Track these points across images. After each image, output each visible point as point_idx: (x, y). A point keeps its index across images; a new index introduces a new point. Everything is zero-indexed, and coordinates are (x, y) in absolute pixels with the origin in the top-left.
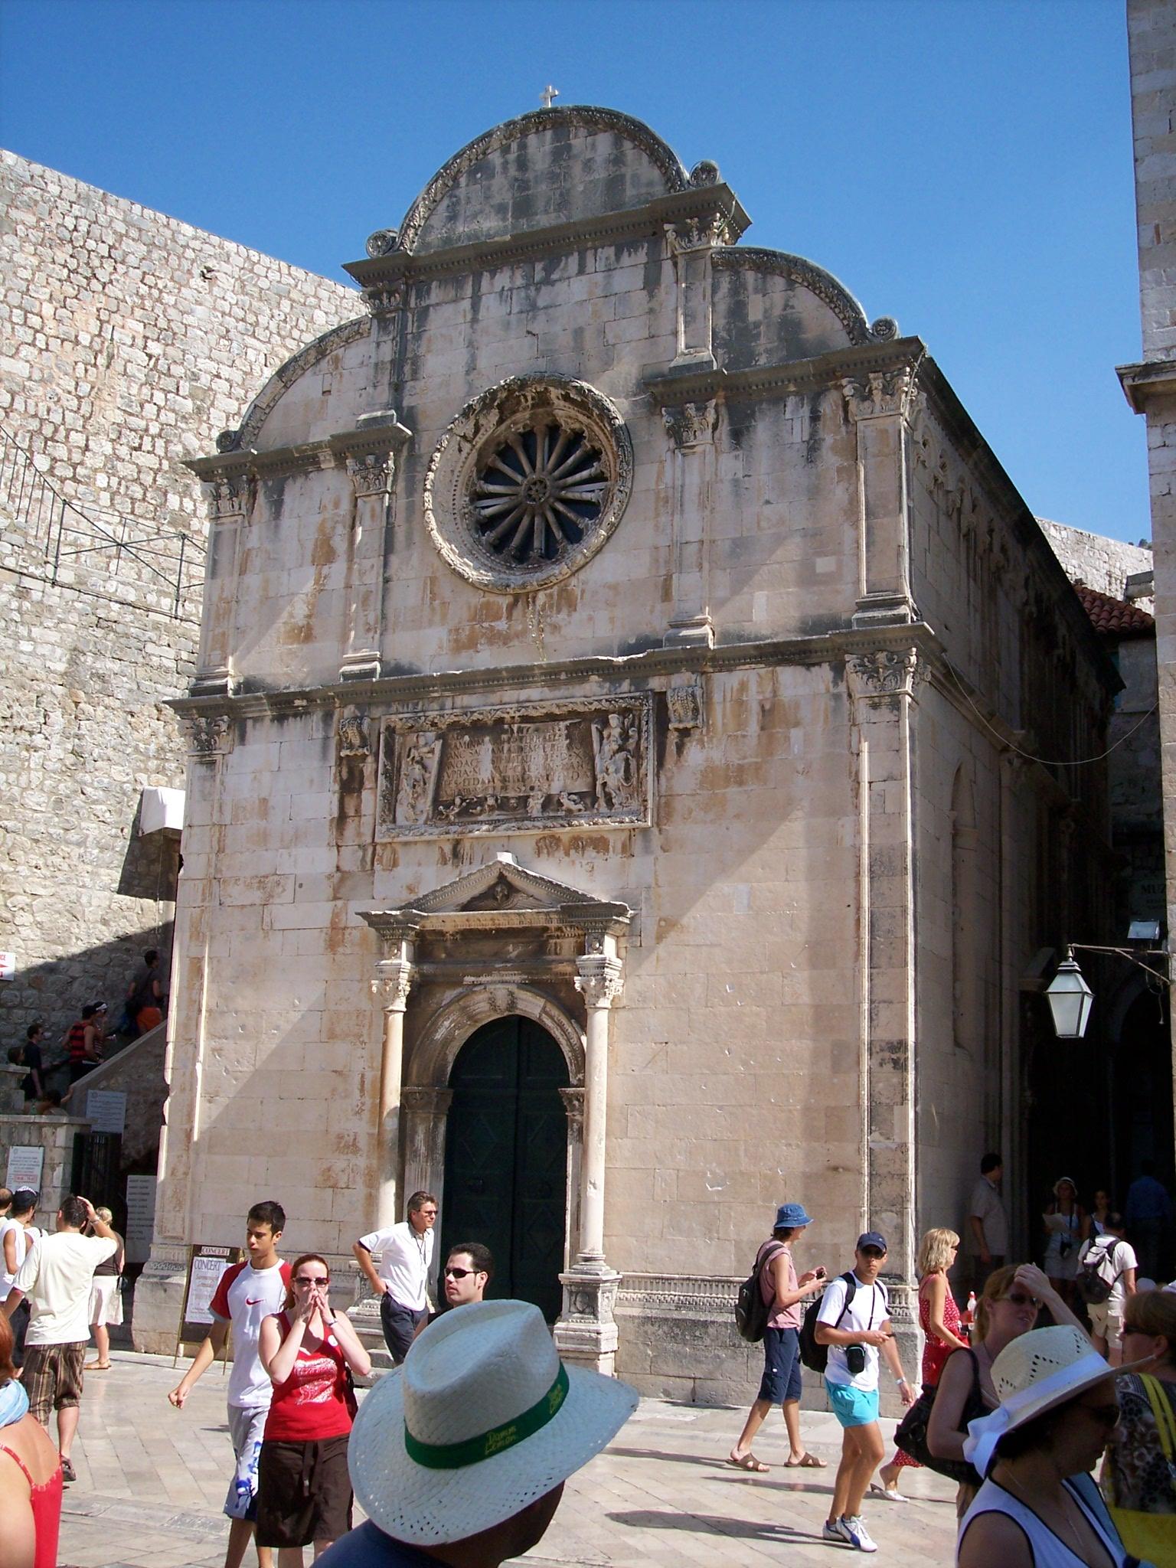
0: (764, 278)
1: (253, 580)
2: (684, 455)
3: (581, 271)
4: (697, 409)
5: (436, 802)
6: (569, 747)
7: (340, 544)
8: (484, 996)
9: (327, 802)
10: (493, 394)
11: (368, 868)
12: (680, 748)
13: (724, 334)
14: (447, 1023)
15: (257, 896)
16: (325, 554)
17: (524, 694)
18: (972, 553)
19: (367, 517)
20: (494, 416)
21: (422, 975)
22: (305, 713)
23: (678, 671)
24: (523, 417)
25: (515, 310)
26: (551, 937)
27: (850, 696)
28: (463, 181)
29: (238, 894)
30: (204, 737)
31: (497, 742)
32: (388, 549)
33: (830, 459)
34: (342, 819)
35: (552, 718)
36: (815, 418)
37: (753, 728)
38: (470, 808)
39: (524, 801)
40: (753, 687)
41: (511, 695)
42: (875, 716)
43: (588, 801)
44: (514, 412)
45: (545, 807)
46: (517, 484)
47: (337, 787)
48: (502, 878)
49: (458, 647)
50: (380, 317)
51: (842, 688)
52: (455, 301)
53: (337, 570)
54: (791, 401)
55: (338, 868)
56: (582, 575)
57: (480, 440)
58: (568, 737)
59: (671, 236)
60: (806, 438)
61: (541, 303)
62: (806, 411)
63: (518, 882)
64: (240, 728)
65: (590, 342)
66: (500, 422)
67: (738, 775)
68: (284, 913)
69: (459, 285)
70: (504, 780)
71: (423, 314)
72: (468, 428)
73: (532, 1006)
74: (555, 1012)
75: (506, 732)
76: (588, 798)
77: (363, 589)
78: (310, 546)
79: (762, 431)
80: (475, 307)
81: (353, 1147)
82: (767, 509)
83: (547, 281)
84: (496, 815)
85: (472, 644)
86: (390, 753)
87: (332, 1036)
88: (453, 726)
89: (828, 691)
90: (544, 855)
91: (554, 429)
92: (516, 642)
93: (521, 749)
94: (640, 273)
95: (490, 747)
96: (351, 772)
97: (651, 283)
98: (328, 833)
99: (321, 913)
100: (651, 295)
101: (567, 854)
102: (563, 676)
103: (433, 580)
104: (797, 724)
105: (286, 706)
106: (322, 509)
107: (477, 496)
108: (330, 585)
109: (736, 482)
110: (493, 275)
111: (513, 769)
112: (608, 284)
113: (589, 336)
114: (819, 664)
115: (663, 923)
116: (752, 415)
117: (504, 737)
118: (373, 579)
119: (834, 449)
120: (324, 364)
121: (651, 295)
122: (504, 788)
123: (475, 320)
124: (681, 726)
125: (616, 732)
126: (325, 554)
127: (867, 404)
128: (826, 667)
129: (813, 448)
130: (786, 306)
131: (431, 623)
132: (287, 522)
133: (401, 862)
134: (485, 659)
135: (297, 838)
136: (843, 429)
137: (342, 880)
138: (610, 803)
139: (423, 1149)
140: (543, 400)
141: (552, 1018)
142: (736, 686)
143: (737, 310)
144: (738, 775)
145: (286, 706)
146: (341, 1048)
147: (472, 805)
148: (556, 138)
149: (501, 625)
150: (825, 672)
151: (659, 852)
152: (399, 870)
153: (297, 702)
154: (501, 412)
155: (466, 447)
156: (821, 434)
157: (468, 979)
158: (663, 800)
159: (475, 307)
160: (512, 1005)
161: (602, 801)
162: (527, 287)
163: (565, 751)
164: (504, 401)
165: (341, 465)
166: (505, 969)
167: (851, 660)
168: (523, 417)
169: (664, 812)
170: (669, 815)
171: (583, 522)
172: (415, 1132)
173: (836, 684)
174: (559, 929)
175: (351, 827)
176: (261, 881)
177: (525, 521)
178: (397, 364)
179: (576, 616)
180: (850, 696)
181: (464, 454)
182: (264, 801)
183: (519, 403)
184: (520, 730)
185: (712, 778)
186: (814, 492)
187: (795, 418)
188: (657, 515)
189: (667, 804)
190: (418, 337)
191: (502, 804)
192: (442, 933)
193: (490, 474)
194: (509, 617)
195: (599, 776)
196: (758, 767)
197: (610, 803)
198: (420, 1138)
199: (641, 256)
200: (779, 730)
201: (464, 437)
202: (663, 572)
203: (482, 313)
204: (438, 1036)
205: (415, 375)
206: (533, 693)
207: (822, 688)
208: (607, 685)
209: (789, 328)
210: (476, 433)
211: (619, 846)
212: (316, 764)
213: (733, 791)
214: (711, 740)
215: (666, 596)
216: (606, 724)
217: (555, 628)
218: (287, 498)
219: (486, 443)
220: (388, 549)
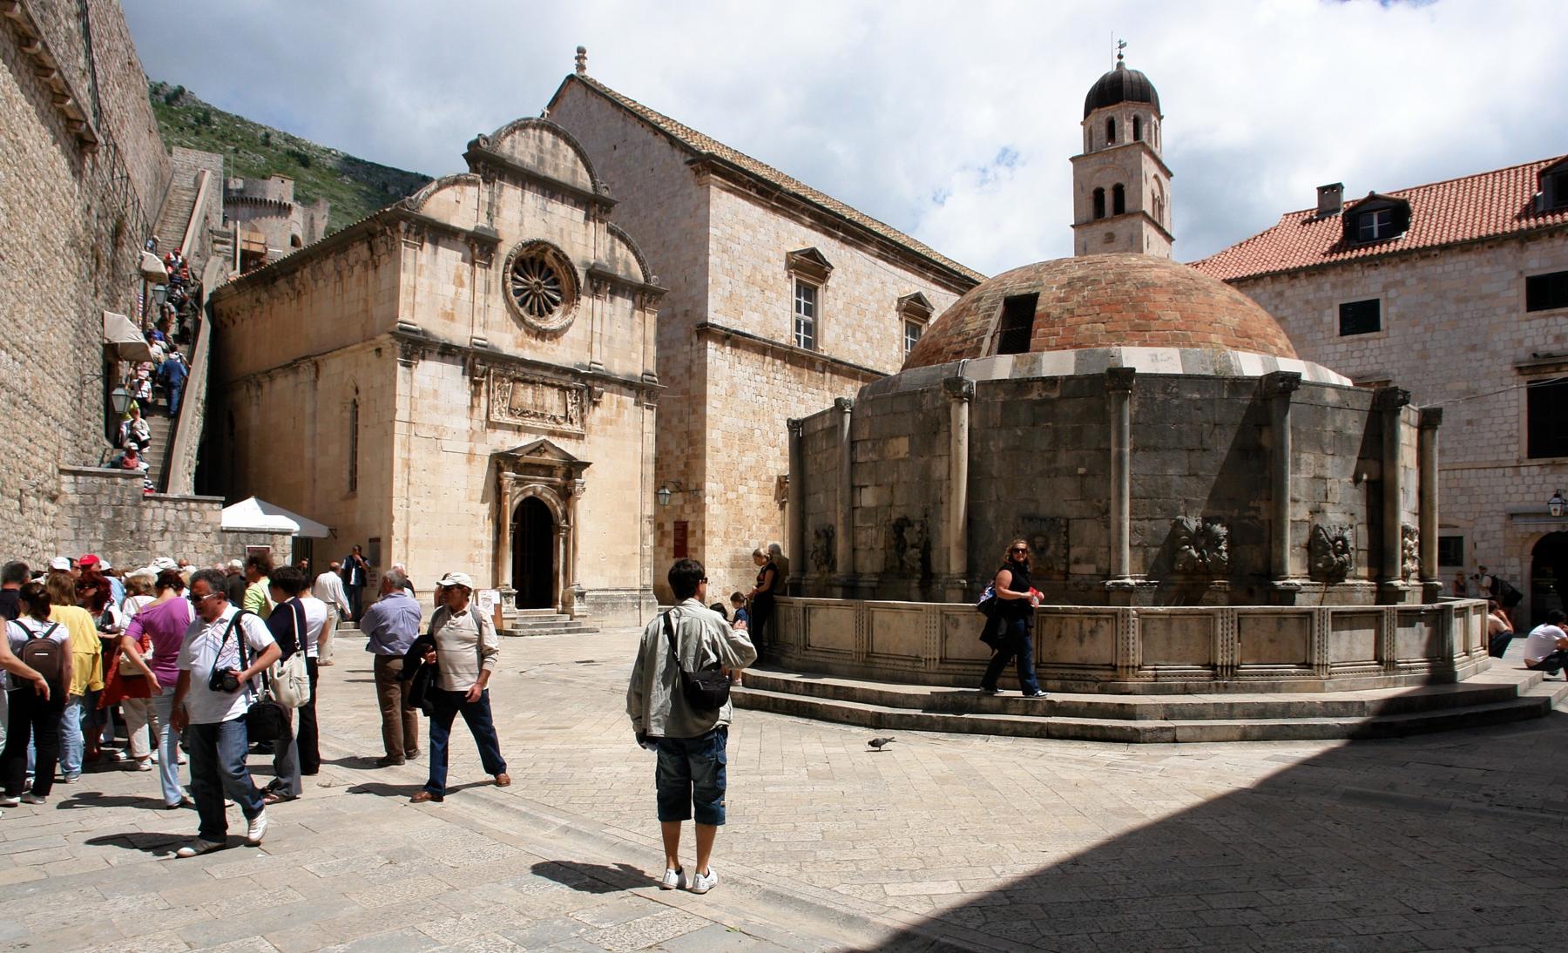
9: (465, 397)
34: (472, 407)
38: (523, 413)
41: (540, 372)
67: (611, 422)
71: (501, 187)
81: (481, 546)
85: (522, 346)
91: (543, 264)
98: (467, 412)
99: (465, 447)
105: (447, 351)
111: (539, 402)
134: (528, 355)
135: (452, 411)
140: (545, 251)
145: (447, 351)
168: (534, 253)
175: (476, 411)
176: (436, 429)
178: (491, 205)
186: (632, 329)
190: (499, 196)
191: (535, 415)
206: (548, 374)
209: (627, 265)
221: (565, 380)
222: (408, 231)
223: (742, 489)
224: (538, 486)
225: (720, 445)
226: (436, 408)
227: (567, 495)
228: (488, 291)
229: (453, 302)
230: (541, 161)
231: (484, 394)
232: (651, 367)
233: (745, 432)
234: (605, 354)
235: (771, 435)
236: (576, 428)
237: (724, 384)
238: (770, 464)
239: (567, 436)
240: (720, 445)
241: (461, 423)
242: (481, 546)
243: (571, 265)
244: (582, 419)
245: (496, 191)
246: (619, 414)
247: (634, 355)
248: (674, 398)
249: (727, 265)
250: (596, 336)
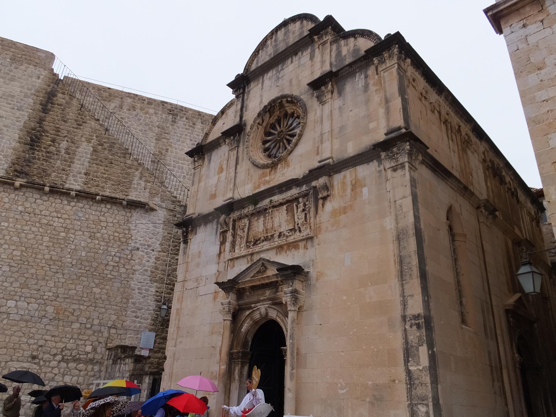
0: (347, 41)
1: (202, 184)
2: (323, 105)
3: (292, 62)
4: (325, 88)
5: (247, 242)
6: (287, 213)
7: (224, 166)
8: (258, 312)
10: (265, 107)
11: (226, 269)
12: (323, 205)
13: (335, 63)
14: (246, 325)
15: (195, 284)
16: (221, 170)
18: (450, 132)
19: (232, 156)
20: (268, 115)
21: (239, 305)
23: (321, 177)
24: (277, 113)
25: (273, 81)
26: (279, 285)
27: (385, 169)
28: (260, 52)
30: (185, 234)
31: (265, 217)
32: (237, 164)
33: (372, 88)
35: (281, 204)
36: (366, 77)
37: (349, 191)
38: (256, 242)
42: (395, 174)
43: (293, 232)
44: (273, 113)
45: (280, 236)
46: (275, 134)
47: (219, 243)
48: (263, 264)
49: (255, 189)
50: (237, 97)
51: (382, 167)
52: (258, 85)
53: (223, 174)
54: (358, 75)
55: (218, 271)
56: (291, 155)
57: (264, 124)
58: (287, 210)
59: (316, 40)
60: (363, 84)
61: (280, 76)
62: (363, 76)
63: (267, 264)
64: (194, 230)
65: (294, 82)
66: (270, 117)
67: (344, 210)
68: (202, 290)
69: (258, 80)
70: (267, 230)
72: (259, 120)
73: (273, 314)
74: (281, 315)
75: (267, 213)
76: (293, 230)
77: (230, 178)
78: (217, 169)
79: (348, 87)
80: (262, 85)
82: (351, 113)
83: (282, 69)
84: (265, 243)
85: (259, 186)
86: (234, 228)
88: (252, 214)
89: (376, 170)
90: (278, 255)
92: (272, 182)
93: (272, 218)
94: (309, 56)
95: (262, 219)
97: (312, 57)
98: (216, 259)
100: (312, 61)
101: (286, 253)
102: (284, 189)
103: (249, 170)
104: (365, 186)
105: (205, 219)
106: (221, 157)
107: (265, 142)
108: (222, 179)
109: (340, 108)
110: (267, 74)
111: (269, 226)
112: (299, 63)
113: (293, 80)
114: (372, 161)
115: (318, 274)
116: (345, 85)
117: (267, 215)
118: (233, 174)
119: (374, 85)
120: (224, 116)
121: (312, 61)
122: (267, 233)
123: (262, 88)
124: (323, 196)
125: (302, 205)
126: (221, 170)
127: (384, 65)
128: (375, 161)
129: (366, 87)
130: (355, 46)
131: (248, 183)
132: (212, 164)
133: (236, 265)
136: (376, 77)
137: (219, 275)
138: (300, 231)
139: (237, 377)
140: (281, 106)
141: (280, 318)
142: (342, 177)
143: (339, 53)
144: (344, 210)
147: (257, 241)
148: (285, 29)
149: (267, 178)
150: (375, 163)
151: (317, 247)
152: (234, 269)
153: (210, 218)
154: (270, 114)
155: (260, 127)
156: (369, 81)
157: (253, 305)
158: (318, 226)
159: (262, 85)
160: (267, 314)
161: (298, 231)
162: (277, 73)
163: (285, 215)
164: (269, 109)
166: (264, 300)
167: (383, 155)
169: (318, 230)
170: (320, 231)
172: (235, 370)
173: (379, 166)
174: (282, 281)
175: (222, 255)
177: (278, 145)
179: (290, 168)
180: (385, 169)
181: (260, 129)
183: (274, 109)
184: (272, 211)
185: (335, 213)
186: (367, 101)
187: (359, 80)
188: (315, 127)
189: (319, 227)
190: (247, 99)
191: (266, 239)
192: (244, 288)
193: (268, 134)
194: (270, 175)
195: (296, 221)
196: (351, 206)
197: (300, 231)
198: (237, 372)
199: (309, 51)
200: (358, 190)
201: (259, 124)
202: (317, 146)
203: (264, 85)
204: (243, 330)
205: (246, 110)
207: (374, 169)
208: (298, 188)
210: (263, 122)
211: (303, 246)
212: (214, 236)
213: (343, 218)
214: (334, 200)
215: (318, 154)
216: (299, 203)
217: (283, 174)
218: (212, 157)
219: (267, 125)
220: (237, 164)
221: (294, 192)
224: (263, 309)
229: (216, 187)
234: (336, 147)
236: (306, 232)
239: (294, 245)
245: (245, 97)
247: (372, 125)
250: (326, 136)
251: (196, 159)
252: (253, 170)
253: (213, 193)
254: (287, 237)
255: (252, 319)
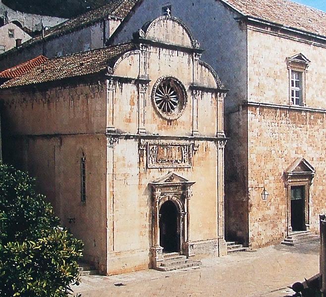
17: (172, 141)
22: (132, 139)
29: (119, 177)
30: (112, 142)
38: (163, 161)
39: (172, 161)
40: (204, 144)
67: (202, 159)
87: (140, 206)
96: (141, 152)
98: (137, 165)
134: (163, 133)
144: (202, 159)
145: (128, 137)
146: (142, 208)
165: (135, 84)
171: (175, 107)
175: (142, 163)
182: (124, 157)
206: (174, 141)
209: (209, 81)
221: (183, 142)
222: (110, 83)
223: (266, 182)
224: (171, 195)
225: (255, 161)
226: (124, 165)
227: (184, 197)
228: (145, 105)
230: (167, 37)
231: (145, 155)
232: (221, 128)
233: (268, 152)
235: (280, 152)
237: (257, 130)
238: (280, 167)
240: (255, 161)
241: (135, 170)
242: (145, 227)
243: (182, 85)
244: (190, 160)
246: (206, 155)
248: (233, 141)
249: (257, 70)
251: (112, 83)
252: (156, 116)
253: (128, 118)
254: (178, 163)
255: (164, 200)
